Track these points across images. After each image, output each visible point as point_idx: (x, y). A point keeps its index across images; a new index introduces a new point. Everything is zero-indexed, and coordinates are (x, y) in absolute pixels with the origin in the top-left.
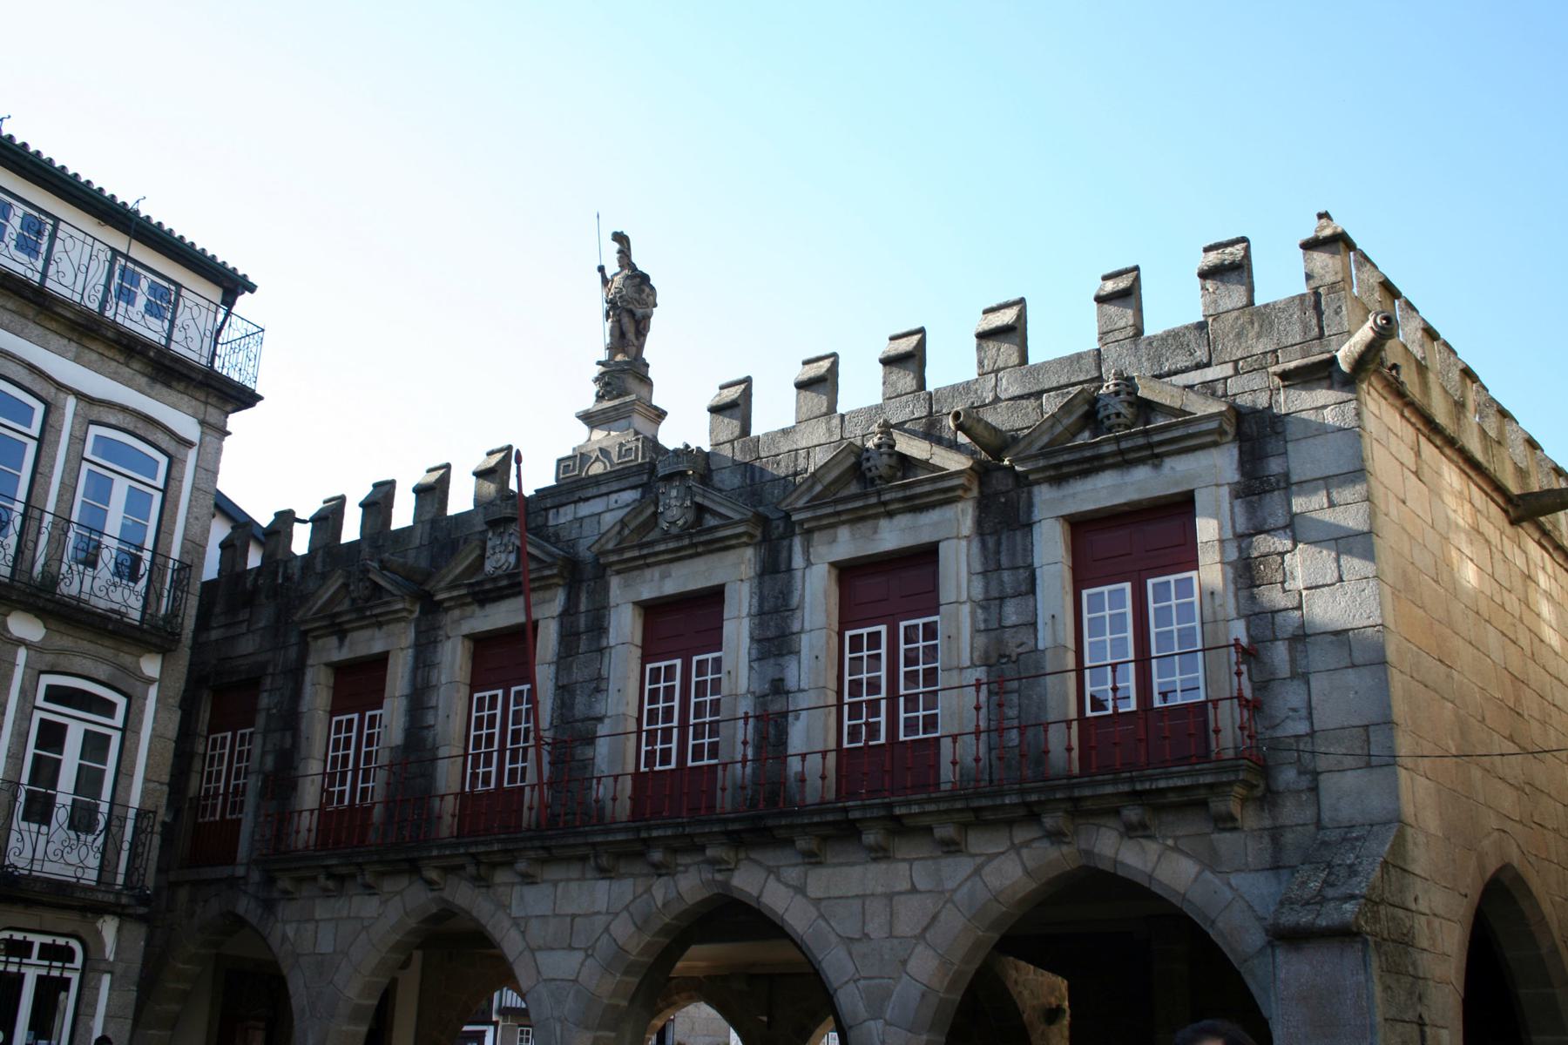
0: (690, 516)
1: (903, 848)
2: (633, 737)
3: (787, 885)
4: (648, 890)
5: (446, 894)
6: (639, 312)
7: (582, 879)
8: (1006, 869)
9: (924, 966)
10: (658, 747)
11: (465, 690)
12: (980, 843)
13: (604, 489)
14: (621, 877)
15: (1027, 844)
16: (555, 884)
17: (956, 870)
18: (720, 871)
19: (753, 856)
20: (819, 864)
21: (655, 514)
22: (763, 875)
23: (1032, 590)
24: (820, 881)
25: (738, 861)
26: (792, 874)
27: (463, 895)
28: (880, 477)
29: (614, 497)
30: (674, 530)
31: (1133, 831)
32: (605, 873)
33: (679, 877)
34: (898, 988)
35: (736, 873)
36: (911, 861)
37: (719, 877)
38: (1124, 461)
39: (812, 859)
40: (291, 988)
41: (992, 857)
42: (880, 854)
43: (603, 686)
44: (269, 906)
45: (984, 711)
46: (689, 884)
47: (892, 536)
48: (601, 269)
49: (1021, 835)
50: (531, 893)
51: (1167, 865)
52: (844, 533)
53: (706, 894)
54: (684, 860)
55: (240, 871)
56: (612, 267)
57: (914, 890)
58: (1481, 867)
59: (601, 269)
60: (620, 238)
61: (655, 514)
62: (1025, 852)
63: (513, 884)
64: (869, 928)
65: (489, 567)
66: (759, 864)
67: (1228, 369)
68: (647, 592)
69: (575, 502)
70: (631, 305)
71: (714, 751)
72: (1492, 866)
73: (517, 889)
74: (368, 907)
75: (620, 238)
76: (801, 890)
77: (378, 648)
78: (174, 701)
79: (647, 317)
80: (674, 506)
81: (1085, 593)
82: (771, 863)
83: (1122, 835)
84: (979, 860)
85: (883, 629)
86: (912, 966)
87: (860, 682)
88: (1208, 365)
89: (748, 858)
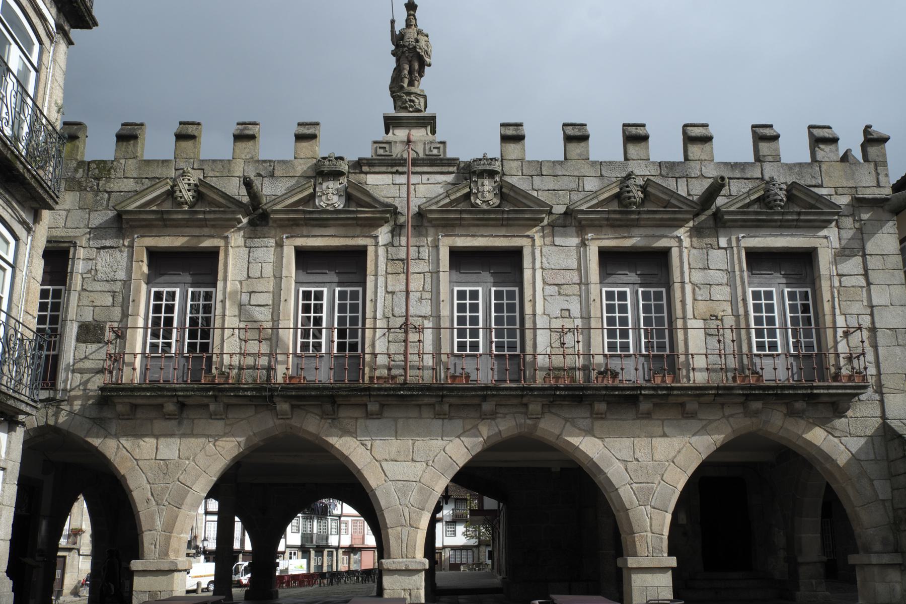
2: (140, 331)
3: (580, 429)
5: (295, 422)
7: (420, 417)
10: (161, 341)
14: (451, 418)
15: (732, 416)
16: (396, 420)
18: (530, 419)
19: (554, 410)
20: (602, 418)
22: (564, 422)
25: (543, 413)
26: (585, 423)
27: (311, 424)
28: (635, 204)
29: (425, 177)
30: (484, 207)
31: (792, 413)
33: (498, 420)
35: (542, 420)
36: (663, 421)
37: (529, 422)
38: (784, 226)
40: (132, 484)
41: (711, 421)
42: (648, 416)
45: (581, 344)
48: (393, 22)
49: (728, 411)
53: (516, 432)
54: (502, 410)
56: (400, 25)
57: (664, 435)
59: (393, 22)
62: (731, 419)
63: (357, 419)
64: (638, 455)
65: (321, 203)
66: (559, 416)
67: (832, 191)
68: (462, 242)
69: (392, 173)
73: (361, 422)
76: (590, 432)
77: (207, 243)
82: (567, 416)
83: (785, 415)
84: (704, 423)
85: (628, 290)
87: (309, 318)
89: (550, 412)
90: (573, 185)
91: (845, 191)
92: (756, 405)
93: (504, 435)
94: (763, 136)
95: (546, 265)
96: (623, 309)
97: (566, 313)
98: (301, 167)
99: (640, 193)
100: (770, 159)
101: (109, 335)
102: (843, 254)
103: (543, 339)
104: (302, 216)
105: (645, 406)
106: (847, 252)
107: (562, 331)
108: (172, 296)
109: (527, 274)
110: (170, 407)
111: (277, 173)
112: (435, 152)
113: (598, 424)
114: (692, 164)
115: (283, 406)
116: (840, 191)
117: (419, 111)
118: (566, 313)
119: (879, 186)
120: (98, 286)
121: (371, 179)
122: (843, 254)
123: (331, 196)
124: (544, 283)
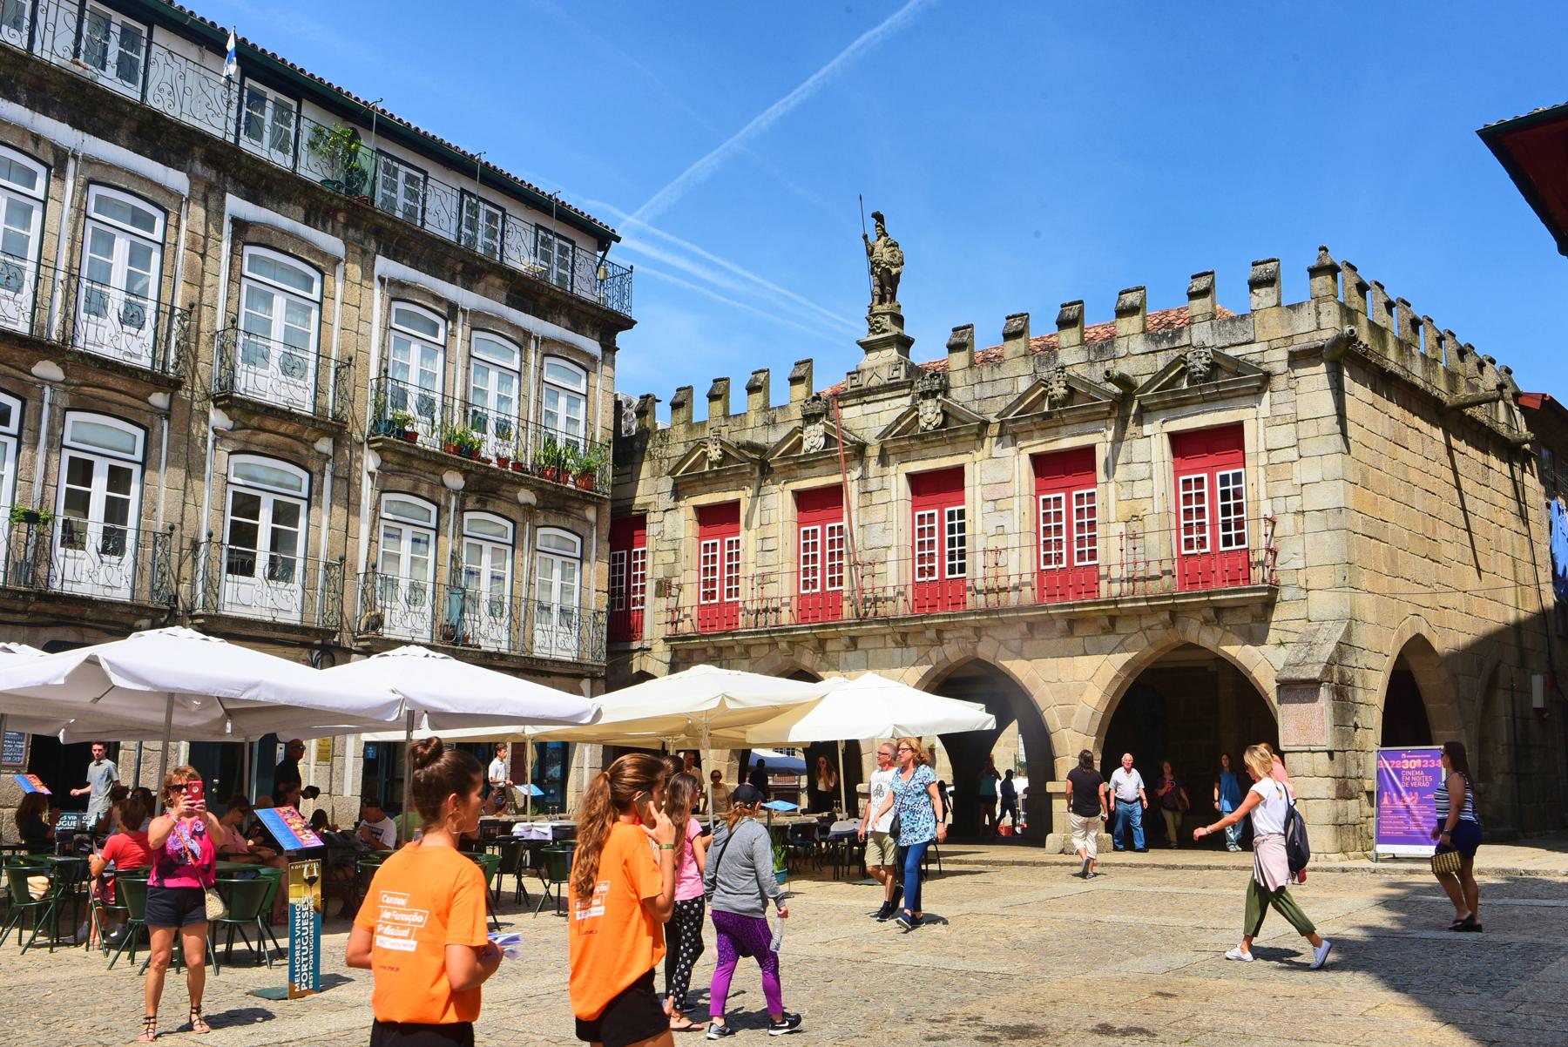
0: (940, 419)
4: (927, 654)
6: (894, 271)
13: (881, 396)
14: (907, 646)
21: (917, 417)
23: (1151, 478)
34: (1078, 710)
41: (1129, 636)
43: (888, 526)
48: (865, 237)
55: (646, 645)
58: (1400, 637)
59: (865, 237)
60: (879, 217)
61: (917, 417)
65: (806, 446)
71: (962, 568)
72: (1408, 635)
75: (879, 217)
77: (730, 496)
78: (606, 537)
79: (898, 274)
80: (930, 413)
81: (1181, 479)
86: (1086, 696)
88: (1252, 342)
90: (1008, 389)
91: (1281, 342)
93: (953, 660)
95: (985, 481)
96: (1058, 515)
97: (1001, 531)
99: (1063, 391)
100: (1200, 318)
101: (674, 591)
104: (795, 460)
106: (1279, 420)
109: (968, 492)
111: (778, 420)
112: (896, 374)
114: (1120, 341)
116: (1275, 344)
117: (885, 331)
118: (1001, 531)
119: (1319, 328)
120: (666, 546)
121: (846, 413)
122: (1272, 422)
123: (814, 437)
124: (984, 500)
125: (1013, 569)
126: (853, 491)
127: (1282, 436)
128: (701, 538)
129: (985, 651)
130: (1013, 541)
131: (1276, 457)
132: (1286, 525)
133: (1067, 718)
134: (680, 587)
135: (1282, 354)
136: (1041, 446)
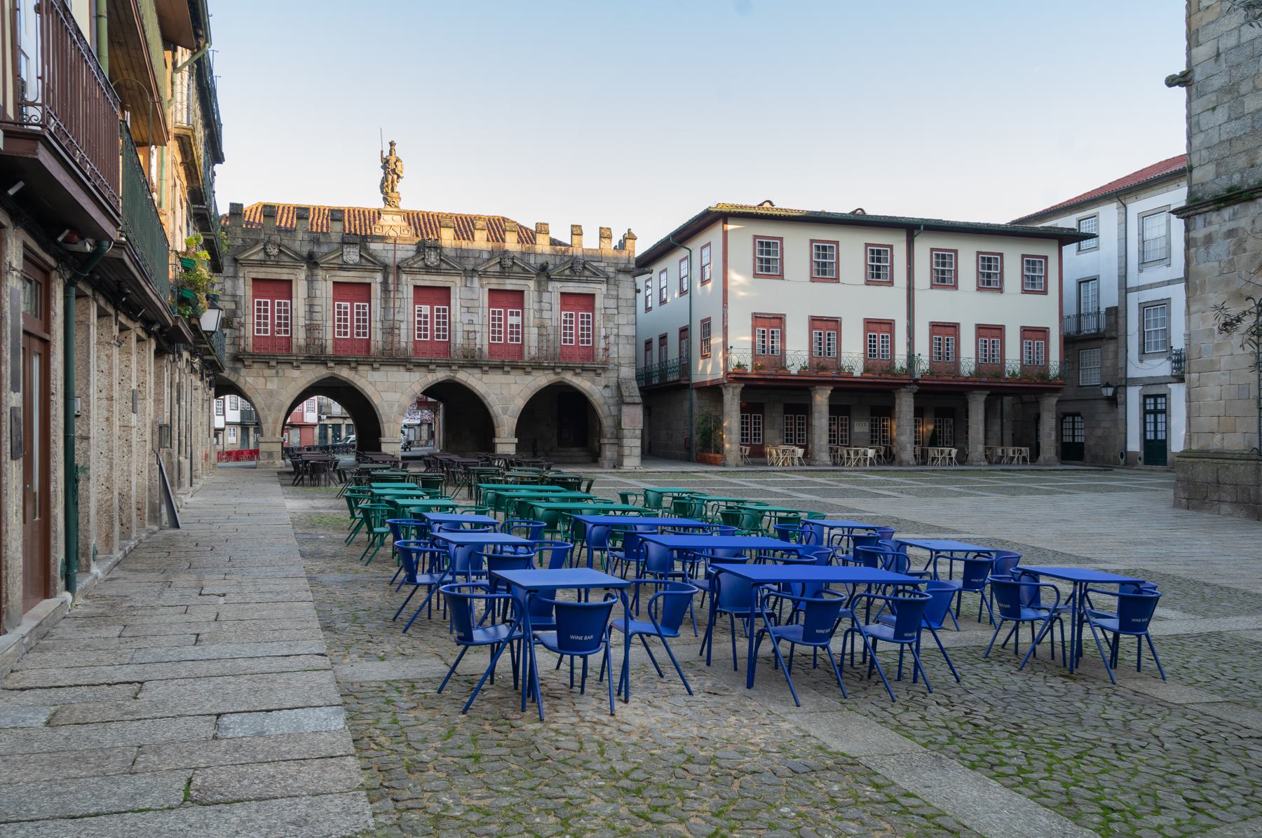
1: (514, 373)
8: (542, 380)
9: (520, 403)
11: (330, 301)
12: (535, 373)
17: (529, 378)
24: (486, 378)
32: (409, 370)
39: (485, 372)
42: (508, 373)
44: (235, 370)
46: (441, 375)
47: (510, 284)
50: (376, 374)
51: (582, 383)
52: (494, 280)
70: (390, 169)
74: (296, 373)
76: (481, 380)
77: (285, 277)
92: (559, 370)
94: (576, 231)
97: (471, 322)
98: (336, 238)
102: (606, 296)
103: (459, 335)
105: (507, 369)
107: (468, 332)
108: (266, 304)
109: (453, 301)
110: (273, 363)
113: (485, 377)
115: (332, 364)
118: (471, 322)
120: (227, 298)
125: (478, 341)
126: (376, 290)
127: (612, 303)
128: (254, 297)
129: (464, 377)
130: (477, 328)
131: (608, 311)
132: (612, 338)
133: (505, 411)
134: (242, 325)
135: (612, 269)
136: (495, 284)
